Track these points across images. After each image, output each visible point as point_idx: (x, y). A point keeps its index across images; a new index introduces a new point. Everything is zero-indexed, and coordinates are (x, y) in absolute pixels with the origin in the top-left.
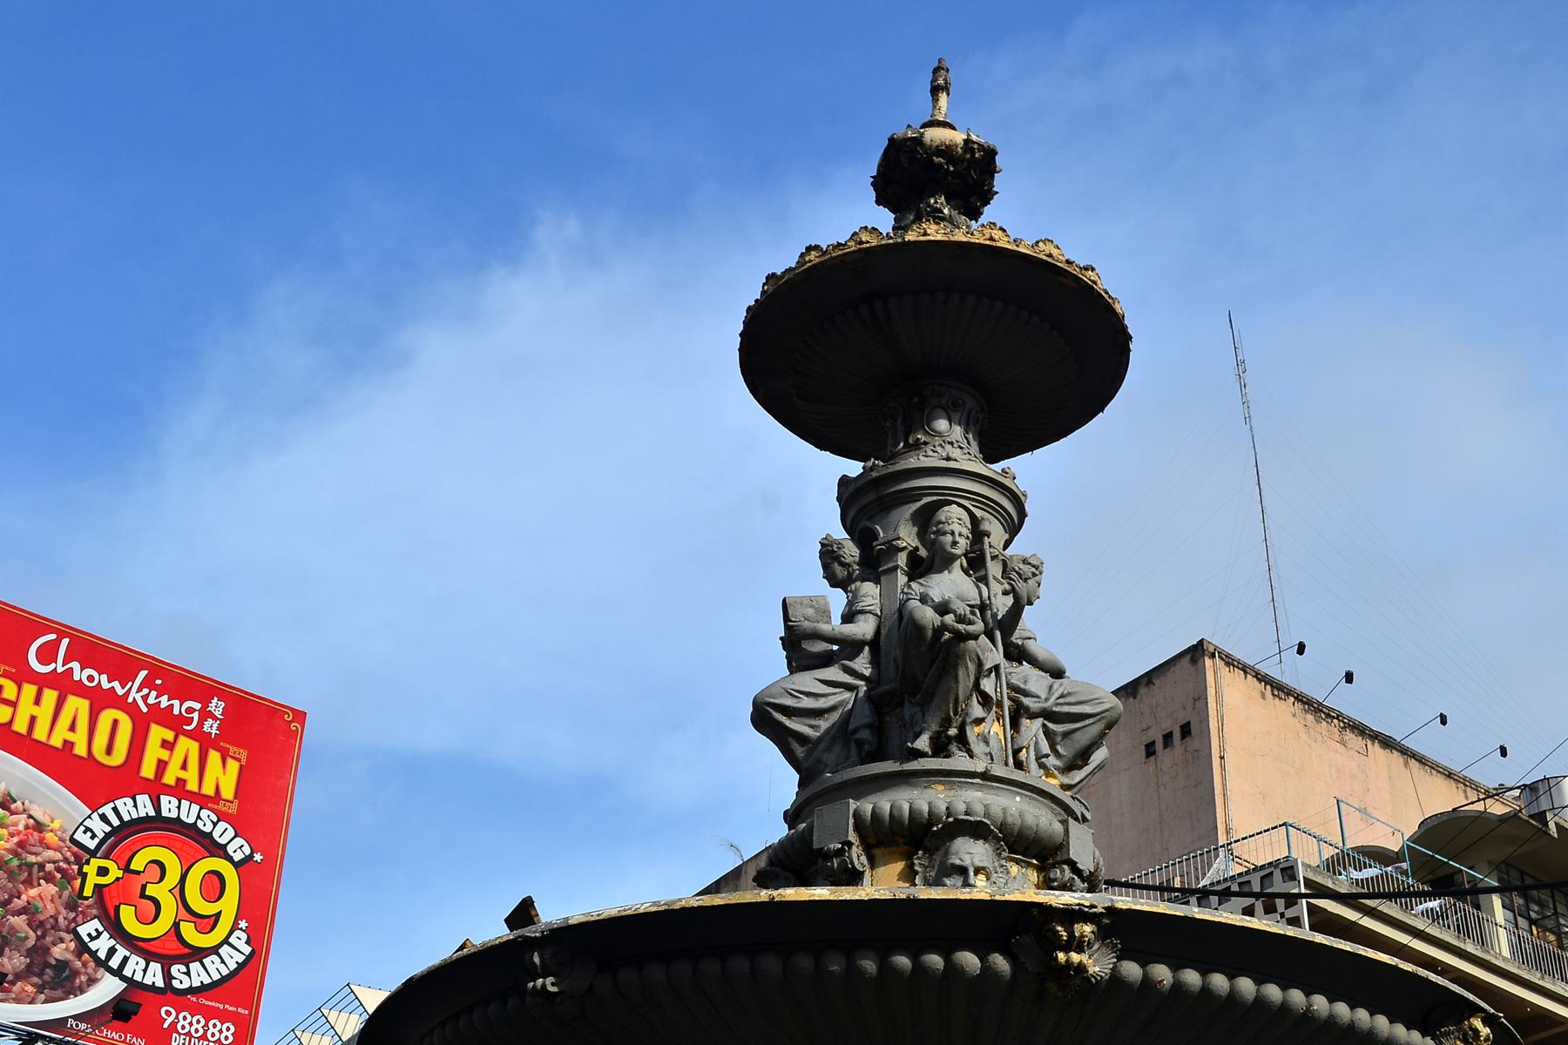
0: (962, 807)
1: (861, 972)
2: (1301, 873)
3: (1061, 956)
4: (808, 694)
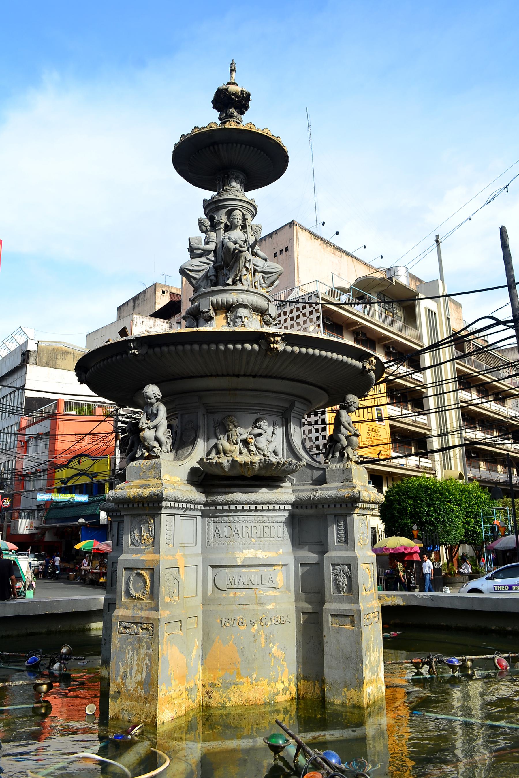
0: (241, 300)
1: (220, 349)
2: (320, 296)
3: (272, 345)
4: (196, 266)
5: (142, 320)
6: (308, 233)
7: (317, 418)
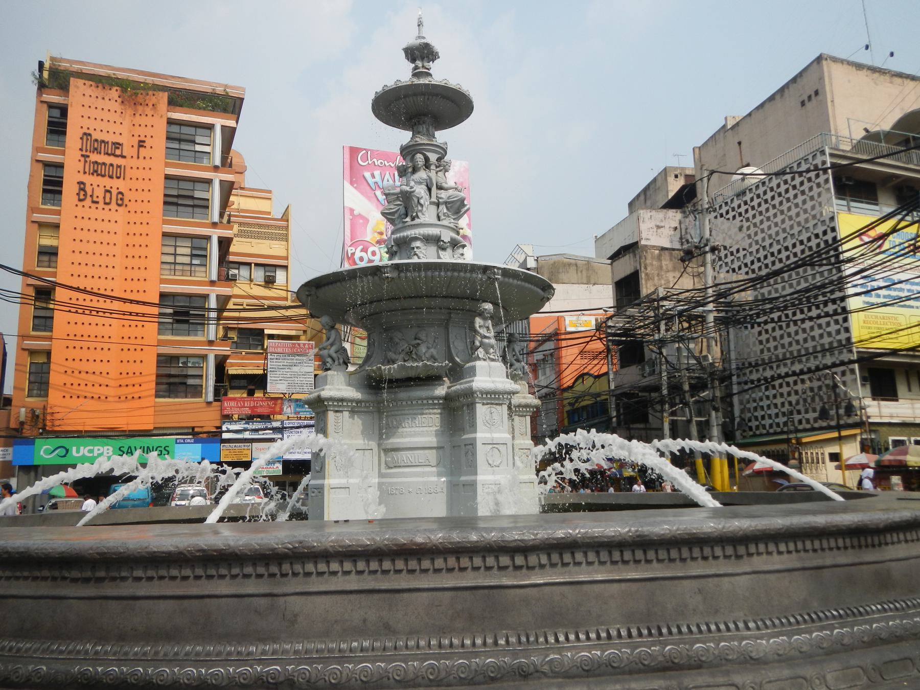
2: (827, 151)
5: (649, 214)
6: (846, 66)
7: (835, 307)
